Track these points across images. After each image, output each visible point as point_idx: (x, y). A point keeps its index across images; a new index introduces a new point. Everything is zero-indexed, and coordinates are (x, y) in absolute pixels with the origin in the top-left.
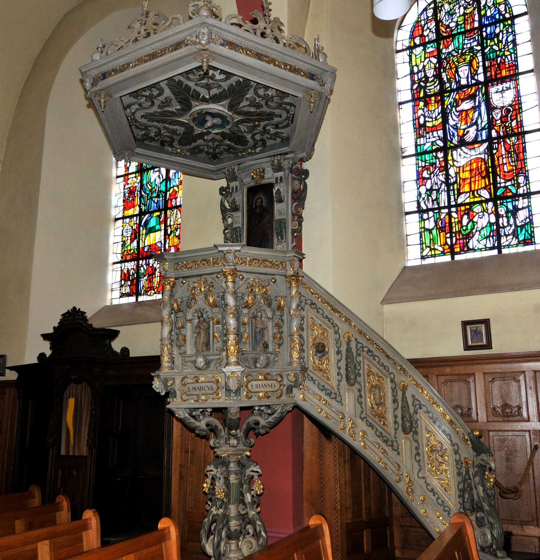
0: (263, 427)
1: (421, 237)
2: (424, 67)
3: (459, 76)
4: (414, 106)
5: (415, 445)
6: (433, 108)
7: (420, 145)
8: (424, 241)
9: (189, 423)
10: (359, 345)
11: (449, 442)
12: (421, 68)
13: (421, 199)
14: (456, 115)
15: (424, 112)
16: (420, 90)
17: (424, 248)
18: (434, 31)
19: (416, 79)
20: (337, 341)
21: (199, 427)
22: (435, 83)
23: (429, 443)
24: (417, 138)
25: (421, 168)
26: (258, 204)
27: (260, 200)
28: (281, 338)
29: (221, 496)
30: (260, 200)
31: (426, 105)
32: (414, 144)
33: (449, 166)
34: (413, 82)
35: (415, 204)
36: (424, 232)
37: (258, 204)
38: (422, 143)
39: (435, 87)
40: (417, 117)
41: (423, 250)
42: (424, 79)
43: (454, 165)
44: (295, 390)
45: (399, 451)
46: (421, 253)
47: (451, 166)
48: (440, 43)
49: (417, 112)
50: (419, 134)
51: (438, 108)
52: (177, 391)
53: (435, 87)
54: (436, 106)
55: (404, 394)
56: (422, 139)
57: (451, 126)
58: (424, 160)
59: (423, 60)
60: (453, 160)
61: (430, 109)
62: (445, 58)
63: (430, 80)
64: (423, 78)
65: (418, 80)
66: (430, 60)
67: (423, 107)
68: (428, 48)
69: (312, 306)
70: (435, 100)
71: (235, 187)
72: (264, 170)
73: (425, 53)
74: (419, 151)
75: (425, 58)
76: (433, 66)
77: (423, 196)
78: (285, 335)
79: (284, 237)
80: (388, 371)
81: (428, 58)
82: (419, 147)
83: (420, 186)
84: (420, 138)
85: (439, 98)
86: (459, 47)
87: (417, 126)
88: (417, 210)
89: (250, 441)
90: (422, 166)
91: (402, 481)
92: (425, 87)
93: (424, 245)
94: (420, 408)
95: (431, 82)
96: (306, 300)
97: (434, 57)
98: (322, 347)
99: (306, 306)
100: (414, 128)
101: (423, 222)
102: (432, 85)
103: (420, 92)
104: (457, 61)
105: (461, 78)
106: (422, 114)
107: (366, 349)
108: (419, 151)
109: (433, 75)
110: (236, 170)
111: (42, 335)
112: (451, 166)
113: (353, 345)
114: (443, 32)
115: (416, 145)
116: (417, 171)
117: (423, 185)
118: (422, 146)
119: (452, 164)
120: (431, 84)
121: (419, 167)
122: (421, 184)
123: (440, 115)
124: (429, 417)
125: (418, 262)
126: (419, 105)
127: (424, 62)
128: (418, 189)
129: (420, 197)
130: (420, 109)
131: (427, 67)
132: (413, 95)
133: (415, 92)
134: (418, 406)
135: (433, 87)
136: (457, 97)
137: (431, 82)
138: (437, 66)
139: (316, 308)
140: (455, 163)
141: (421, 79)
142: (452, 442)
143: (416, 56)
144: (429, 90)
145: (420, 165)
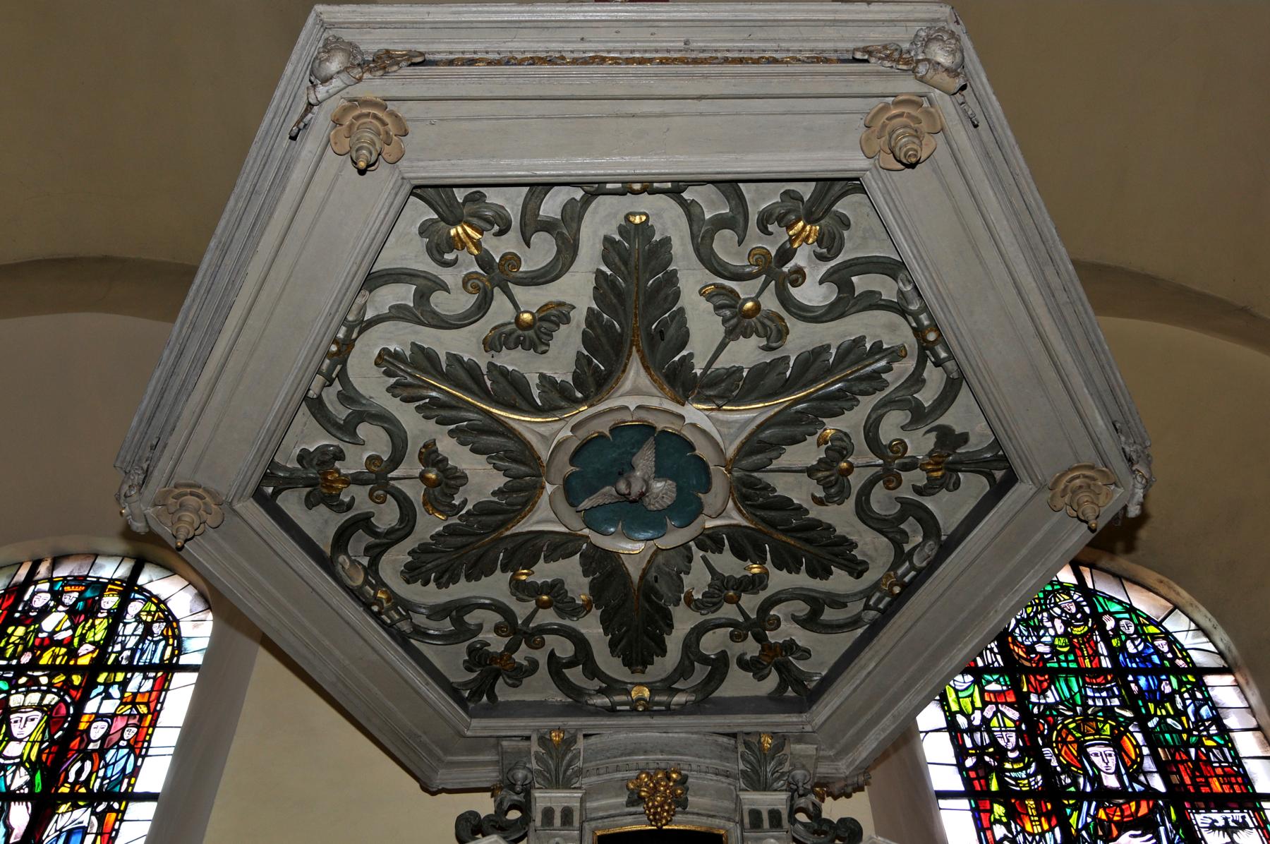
2: (986, 721)
6: (1038, 829)
12: (977, 722)
18: (996, 650)
19: (969, 744)
22: (1027, 766)
31: (1014, 814)
39: (1029, 776)
48: (1021, 680)
51: (1051, 829)
53: (1029, 776)
54: (1046, 827)
59: (978, 704)
61: (1028, 827)
62: (1041, 715)
66: (998, 710)
67: (1004, 820)
68: (989, 682)
70: (1037, 809)
72: (683, 781)
73: (982, 691)
75: (985, 704)
81: (991, 703)
86: (1072, 697)
92: (1001, 772)
95: (1014, 761)
97: (1011, 705)
109: (1017, 747)
126: (991, 811)
127: (982, 710)
131: (994, 723)
135: (1023, 775)
137: (1014, 761)
138: (1023, 727)
143: (957, 691)
144: (1015, 779)
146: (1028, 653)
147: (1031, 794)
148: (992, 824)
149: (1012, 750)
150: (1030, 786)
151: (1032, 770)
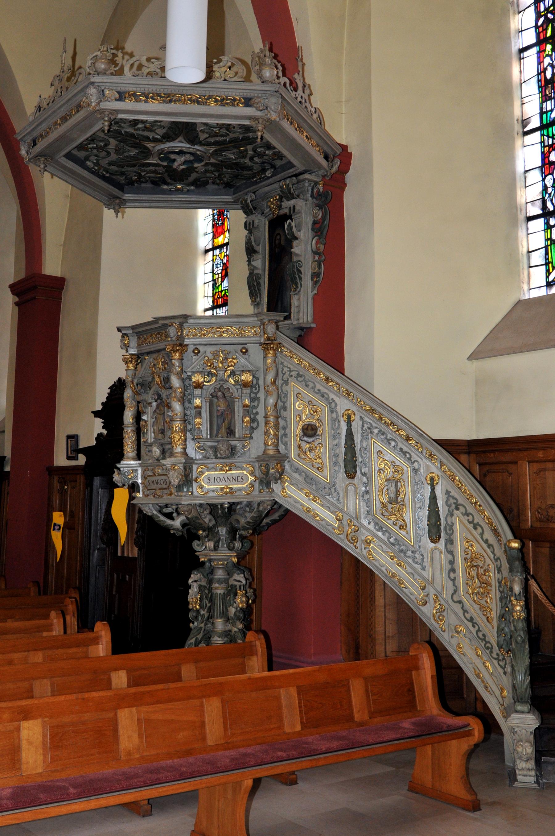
0: (244, 529)
1: (547, 253)
4: (539, 53)
5: (450, 557)
7: (546, 112)
8: (550, 260)
9: (158, 521)
10: (366, 426)
11: (492, 556)
13: (547, 195)
15: (552, 60)
16: (548, 26)
17: (551, 270)
19: (542, 9)
20: (335, 421)
21: (172, 526)
23: (468, 556)
24: (543, 102)
25: (547, 148)
26: (277, 242)
27: (278, 237)
28: (253, 420)
29: (193, 607)
30: (278, 237)
32: (539, 112)
34: (538, 15)
35: (539, 203)
36: (550, 245)
37: (277, 242)
38: (549, 108)
40: (542, 70)
41: (550, 274)
42: (552, 8)
44: (274, 486)
45: (425, 564)
46: (547, 277)
49: (543, 62)
50: (546, 95)
52: (140, 485)
55: (433, 489)
56: (549, 102)
58: (551, 135)
64: (551, 6)
65: (544, 11)
67: (550, 53)
69: (299, 379)
71: (251, 222)
74: (545, 122)
77: (550, 190)
78: (260, 418)
79: (299, 286)
80: (410, 459)
82: (544, 116)
83: (546, 176)
84: (546, 101)
87: (543, 83)
88: (541, 212)
89: (234, 544)
90: (548, 145)
91: (428, 604)
93: (550, 265)
94: (457, 509)
96: (290, 371)
98: (312, 429)
99: (290, 379)
100: (539, 87)
101: (549, 230)
103: (546, 29)
106: (549, 63)
107: (376, 431)
108: (545, 122)
110: (249, 201)
111: (92, 412)
113: (356, 426)
115: (542, 113)
116: (543, 153)
117: (549, 174)
118: (549, 113)
121: (545, 147)
122: (546, 173)
124: (468, 520)
125: (543, 292)
126: (545, 51)
128: (543, 180)
129: (546, 192)
130: (547, 55)
132: (538, 35)
133: (541, 29)
134: (454, 506)
139: (304, 380)
141: (549, 7)
142: (495, 555)
145: (546, 144)
148: (544, 58)
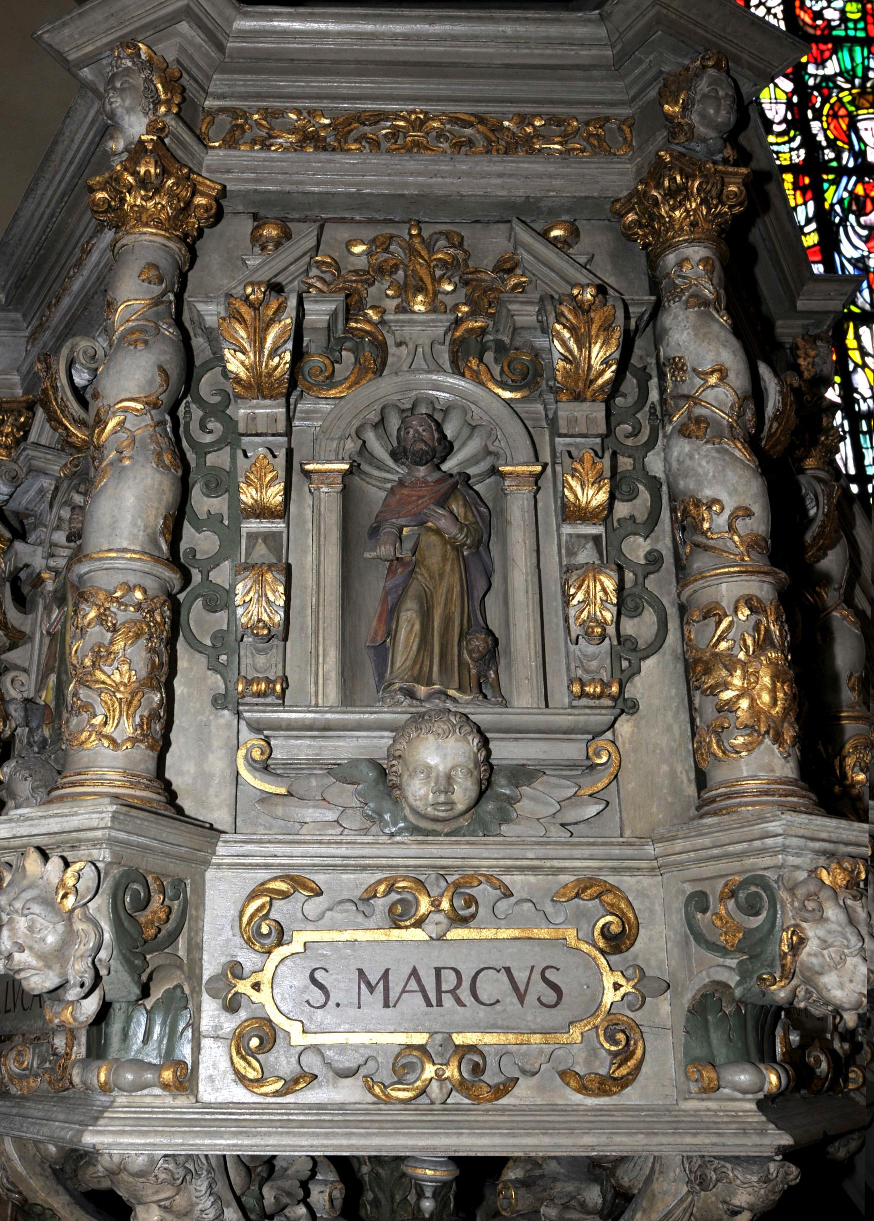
3: (860, 139)
14: (860, 237)
33: (851, 367)
39: (791, 150)
43: (864, 366)
47: (856, 365)
51: (805, 203)
53: (791, 150)
57: (849, 260)
60: (864, 353)
62: (816, 87)
63: (777, 128)
70: (794, 183)
76: (783, 98)
85: (807, 181)
86: (854, 69)
95: (780, 134)
102: (784, 143)
104: (851, 103)
105: (866, 145)
109: (785, 120)
112: (856, 365)
114: (805, 23)
119: (860, 362)
120: (780, 140)
123: (813, 226)
136: (860, 190)
137: (780, 134)
138: (795, 99)
140: (868, 360)
144: (777, 153)
146: (814, 19)
147: (792, 168)
149: (780, 123)
150: (791, 160)
151: (795, 145)
